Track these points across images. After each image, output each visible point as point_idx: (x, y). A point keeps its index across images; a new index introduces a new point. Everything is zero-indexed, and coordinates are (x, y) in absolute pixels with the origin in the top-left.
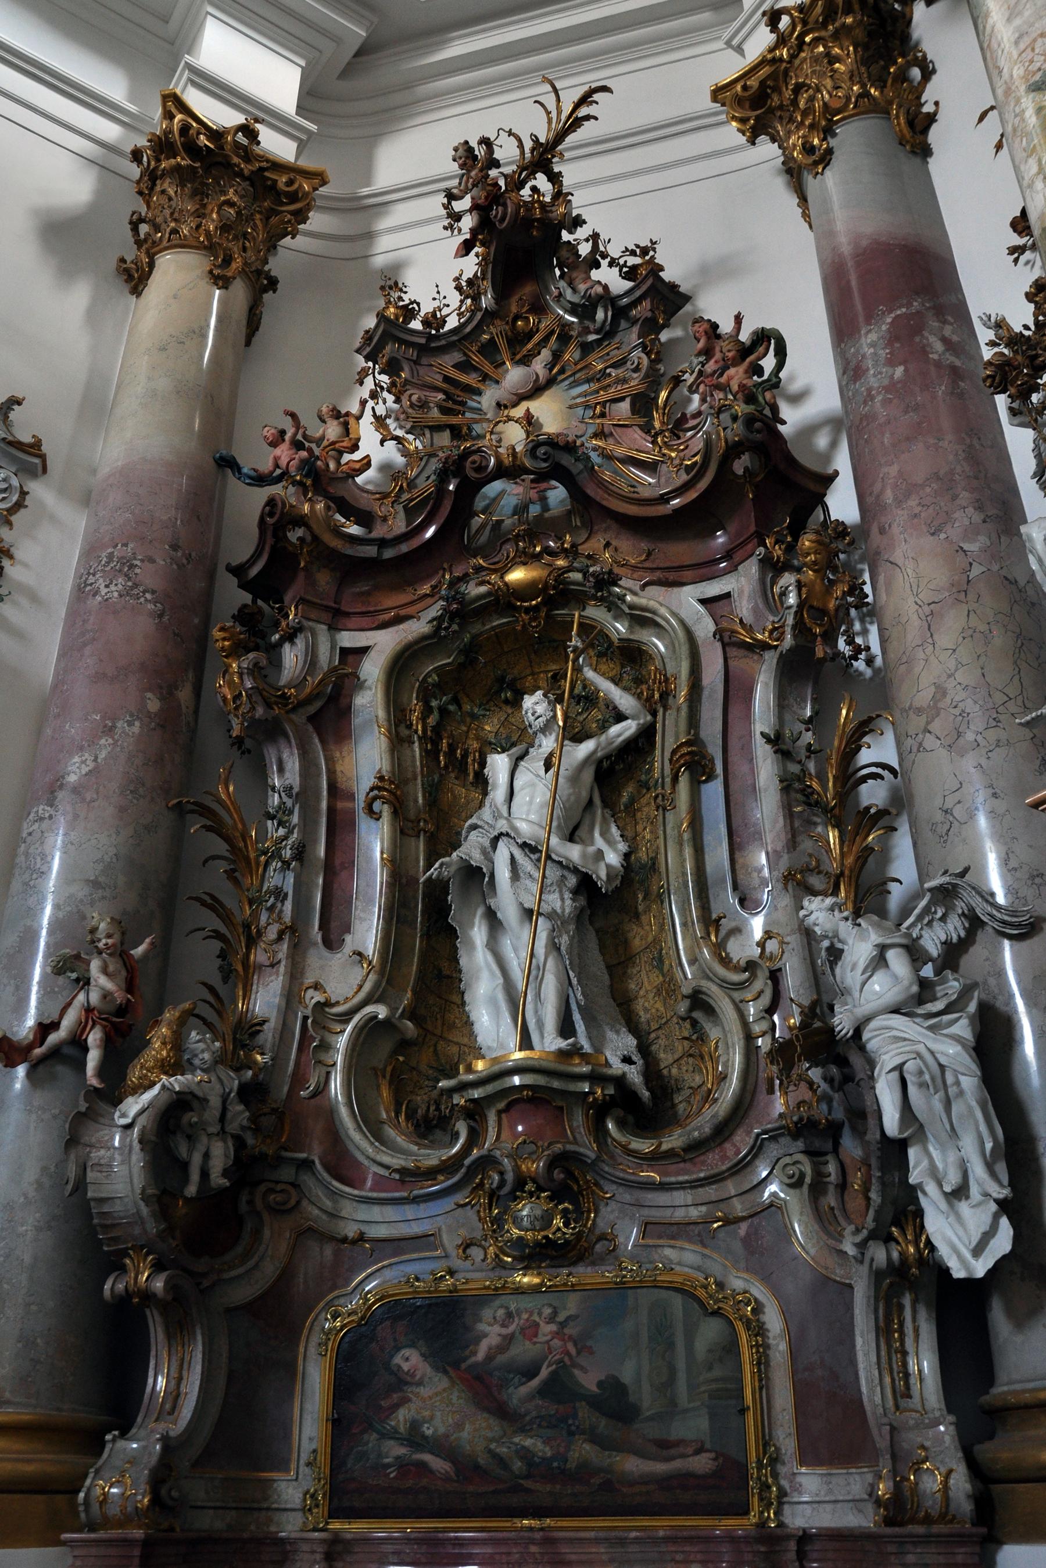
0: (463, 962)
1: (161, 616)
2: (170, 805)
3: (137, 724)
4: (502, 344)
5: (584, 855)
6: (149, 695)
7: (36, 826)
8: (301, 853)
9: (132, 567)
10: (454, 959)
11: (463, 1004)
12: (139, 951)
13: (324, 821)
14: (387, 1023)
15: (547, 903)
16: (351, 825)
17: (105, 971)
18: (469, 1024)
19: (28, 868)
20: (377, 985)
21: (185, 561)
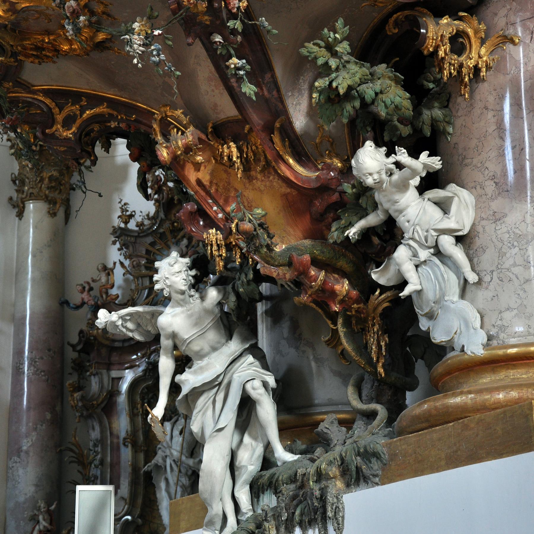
0: (158, 495)
1: (47, 380)
2: (58, 451)
3: (44, 425)
4: (168, 234)
5: (194, 463)
6: (47, 413)
7: (14, 465)
8: (102, 462)
9: (35, 362)
10: (154, 494)
11: (158, 510)
12: (53, 507)
13: (109, 447)
14: (133, 521)
15: (180, 481)
16: (118, 449)
17: (44, 520)
18: (160, 516)
19: (14, 479)
20: (128, 508)
21: (53, 355)
